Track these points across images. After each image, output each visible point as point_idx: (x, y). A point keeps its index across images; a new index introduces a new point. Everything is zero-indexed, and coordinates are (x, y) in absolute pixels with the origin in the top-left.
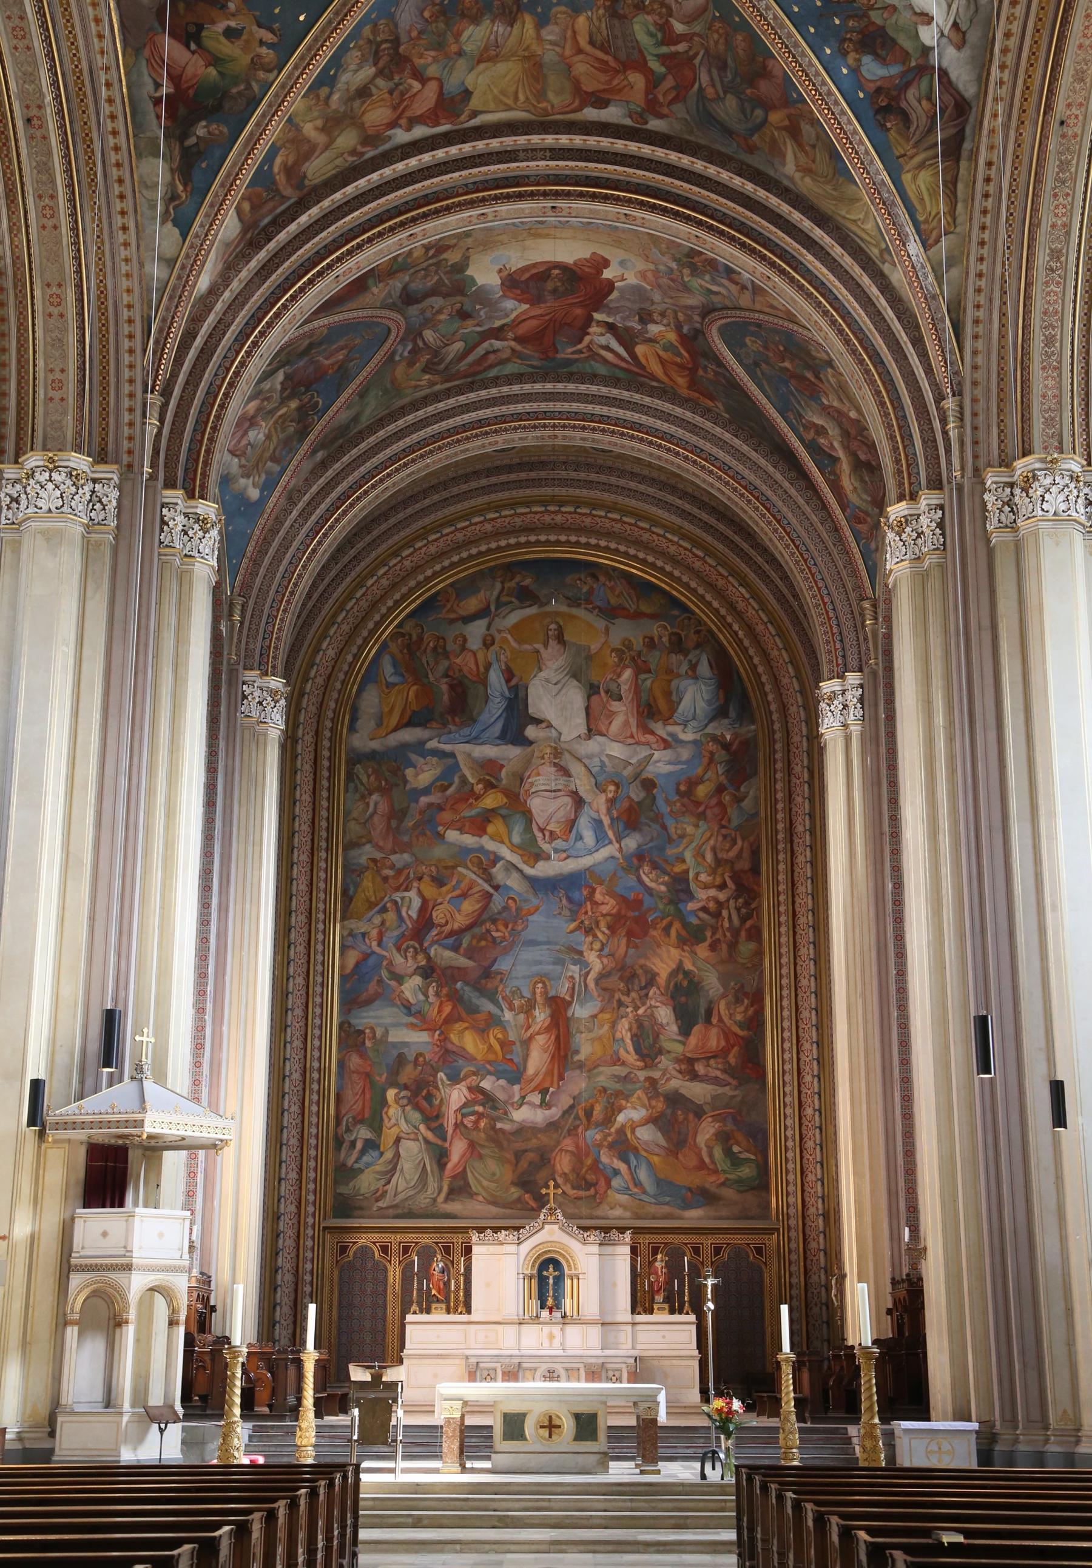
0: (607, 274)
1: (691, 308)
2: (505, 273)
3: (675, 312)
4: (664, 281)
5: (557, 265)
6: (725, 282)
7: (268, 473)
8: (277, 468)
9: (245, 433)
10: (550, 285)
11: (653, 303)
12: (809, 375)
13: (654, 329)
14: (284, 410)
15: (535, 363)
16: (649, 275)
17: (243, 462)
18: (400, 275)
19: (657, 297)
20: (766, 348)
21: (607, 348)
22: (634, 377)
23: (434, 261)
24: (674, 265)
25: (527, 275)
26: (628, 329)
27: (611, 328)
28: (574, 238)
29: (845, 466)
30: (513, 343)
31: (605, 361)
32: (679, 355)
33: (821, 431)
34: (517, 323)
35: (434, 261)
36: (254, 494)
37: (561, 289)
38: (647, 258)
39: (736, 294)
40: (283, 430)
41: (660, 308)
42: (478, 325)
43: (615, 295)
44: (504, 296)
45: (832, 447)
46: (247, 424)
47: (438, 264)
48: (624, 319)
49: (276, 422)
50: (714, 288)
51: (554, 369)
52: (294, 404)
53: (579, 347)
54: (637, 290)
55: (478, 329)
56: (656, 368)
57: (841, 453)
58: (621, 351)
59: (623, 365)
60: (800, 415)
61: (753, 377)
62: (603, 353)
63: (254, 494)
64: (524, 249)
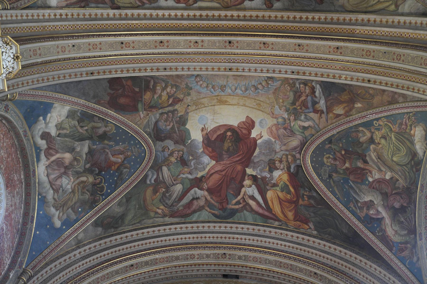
0: (254, 134)
1: (295, 148)
2: (205, 132)
3: (287, 155)
4: (282, 131)
5: (230, 128)
6: (312, 115)
7: (68, 216)
8: (73, 217)
9: (60, 177)
10: (227, 145)
11: (276, 153)
12: (360, 164)
13: (277, 174)
14: (84, 179)
15: (216, 212)
16: (274, 129)
17: (56, 197)
18: (154, 110)
19: (277, 147)
20: (335, 159)
21: (253, 198)
22: (267, 217)
23: (170, 108)
24: (286, 116)
25: (215, 136)
26: (263, 179)
27: (254, 178)
28: (238, 104)
29: (388, 221)
30: (206, 193)
31: (252, 210)
32: (289, 192)
33: (370, 205)
34: (210, 175)
35: (170, 108)
36: (58, 224)
37: (231, 148)
38: (273, 115)
39: (317, 121)
40: (83, 193)
41: (279, 156)
42: (190, 173)
43: (257, 151)
44: (203, 152)
45: (378, 212)
46: (62, 170)
47: (173, 112)
48: (261, 171)
49: (79, 184)
50: (306, 124)
51: (226, 215)
52: (91, 179)
53: (239, 198)
54: (268, 143)
55: (190, 177)
56: (277, 209)
57: (384, 213)
58: (259, 198)
59: (261, 211)
60: (357, 201)
61: (328, 186)
62: (251, 202)
63: (58, 224)
64: (215, 113)
